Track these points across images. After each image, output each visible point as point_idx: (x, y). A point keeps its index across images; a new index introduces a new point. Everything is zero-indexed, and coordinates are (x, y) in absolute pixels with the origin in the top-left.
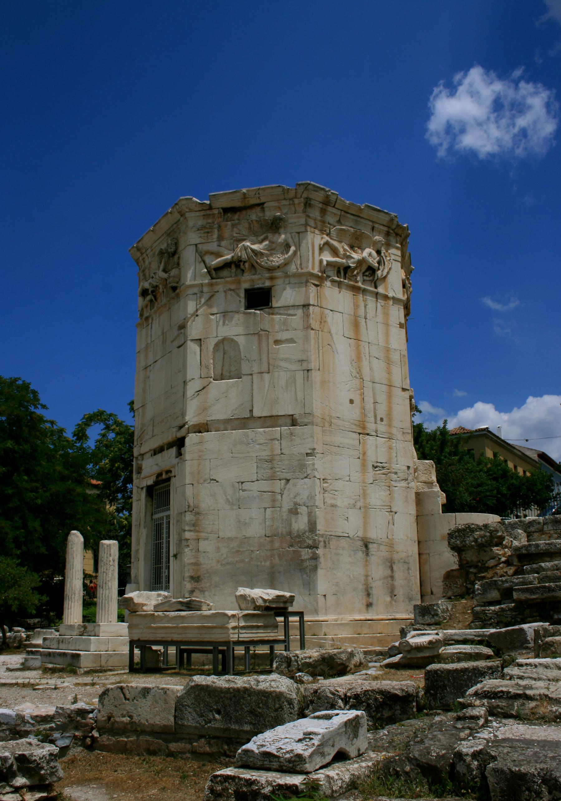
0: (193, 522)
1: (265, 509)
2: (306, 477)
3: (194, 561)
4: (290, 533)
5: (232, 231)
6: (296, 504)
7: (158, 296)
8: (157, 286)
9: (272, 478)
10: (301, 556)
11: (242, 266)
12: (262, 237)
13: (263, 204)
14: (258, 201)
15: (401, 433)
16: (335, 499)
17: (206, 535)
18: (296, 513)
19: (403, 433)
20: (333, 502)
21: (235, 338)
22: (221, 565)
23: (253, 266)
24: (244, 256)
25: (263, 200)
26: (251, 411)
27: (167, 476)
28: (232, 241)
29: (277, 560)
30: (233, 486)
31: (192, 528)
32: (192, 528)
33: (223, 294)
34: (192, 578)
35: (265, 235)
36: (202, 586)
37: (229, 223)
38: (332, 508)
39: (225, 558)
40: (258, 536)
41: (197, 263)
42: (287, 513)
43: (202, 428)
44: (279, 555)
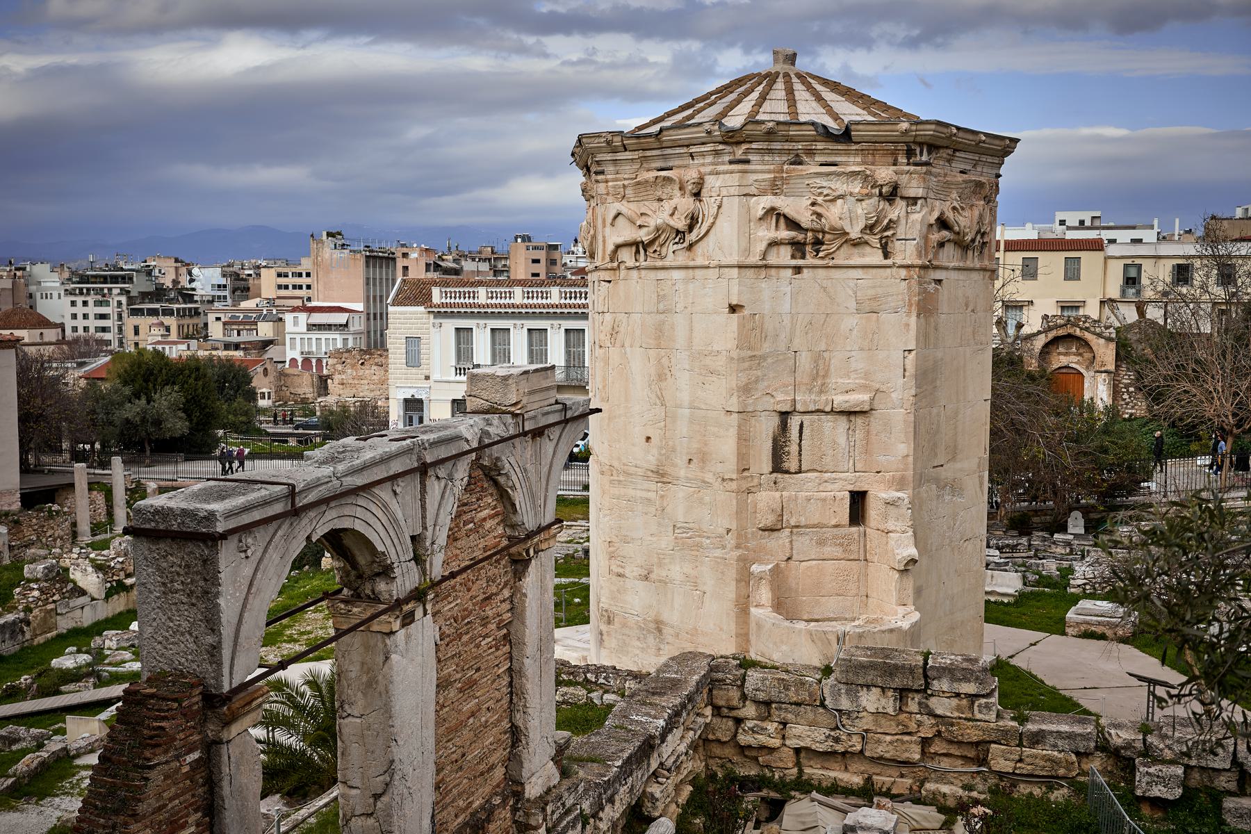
19: (723, 480)
20: (621, 570)
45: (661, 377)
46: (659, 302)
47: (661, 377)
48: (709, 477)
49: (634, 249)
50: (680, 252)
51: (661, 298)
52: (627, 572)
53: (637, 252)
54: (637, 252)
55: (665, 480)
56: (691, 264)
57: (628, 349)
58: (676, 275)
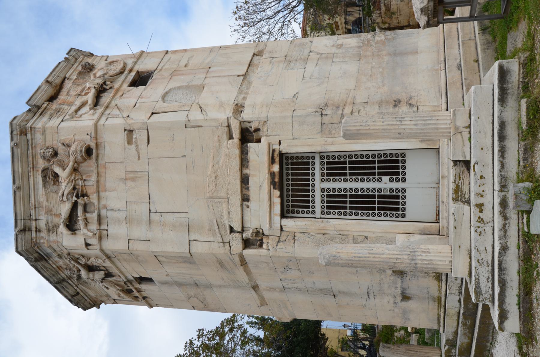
0: (334, 108)
1: (333, 62)
2: (312, 42)
3: (377, 105)
4: (359, 47)
6: (334, 45)
8: (74, 188)
10: (382, 40)
11: (108, 87)
21: (167, 90)
22: (383, 85)
24: (100, 81)
26: (238, 76)
27: (277, 160)
29: (384, 53)
32: (341, 108)
36: (405, 99)
43: (239, 109)
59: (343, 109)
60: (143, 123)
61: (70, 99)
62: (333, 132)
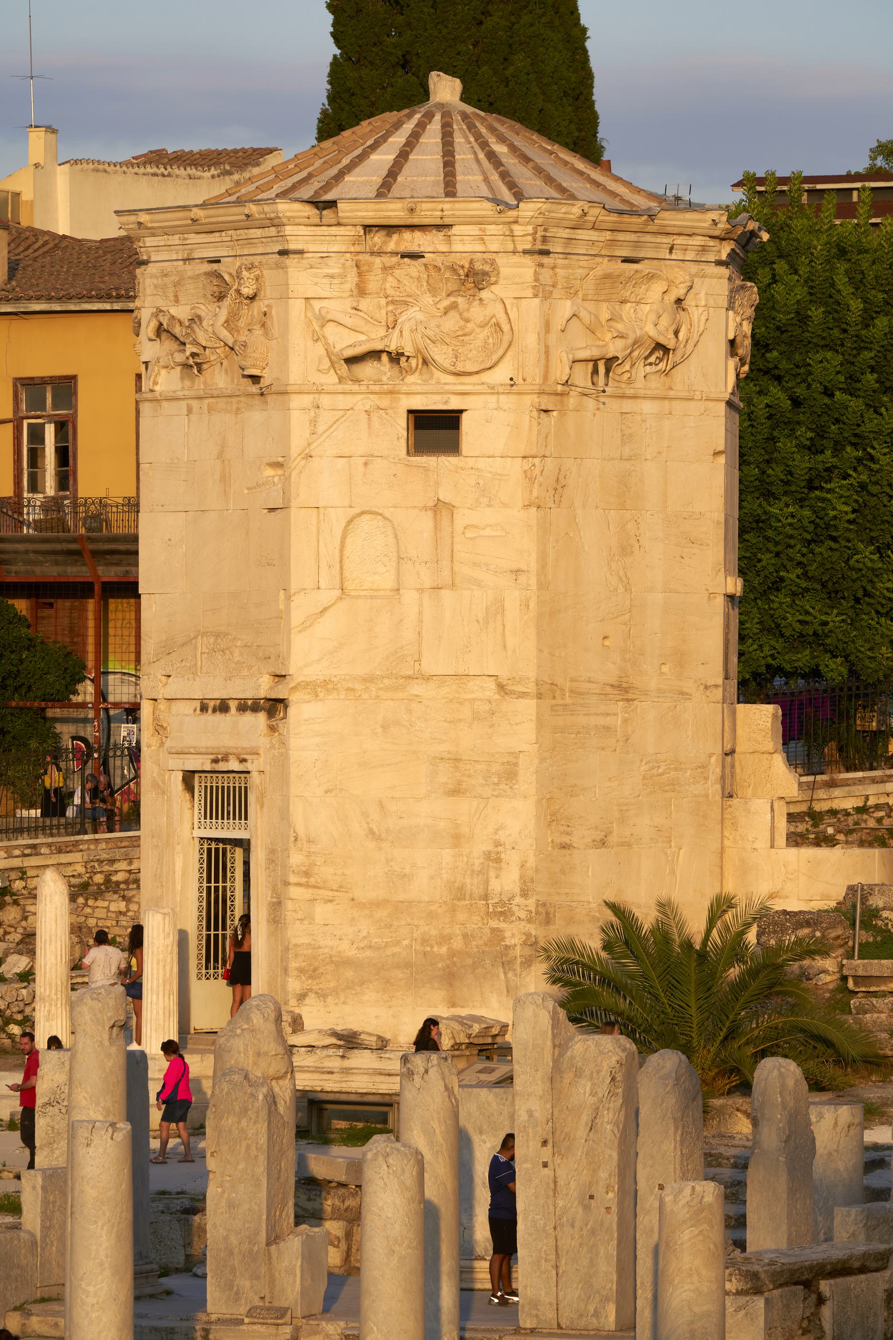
0: (304, 869)
4: (486, 897)
5: (384, 280)
6: (497, 844)
7: (205, 366)
9: (455, 791)
10: (503, 939)
12: (446, 303)
13: (449, 226)
14: (439, 222)
15: (702, 687)
16: (568, 834)
17: (331, 893)
18: (498, 860)
19: (706, 687)
20: (566, 839)
23: (425, 362)
25: (447, 221)
28: (383, 301)
30: (381, 805)
31: (304, 880)
32: (304, 880)
33: (364, 416)
34: (301, 970)
35: (452, 299)
37: (378, 261)
38: (564, 851)
39: (365, 938)
40: (427, 899)
41: (310, 343)
42: (481, 860)
44: (465, 936)
45: (625, 550)
46: (623, 443)
47: (625, 550)
48: (689, 686)
49: (591, 364)
50: (653, 377)
51: (627, 438)
52: (576, 840)
53: (595, 371)
54: (595, 371)
55: (630, 696)
56: (672, 394)
57: (579, 512)
58: (648, 407)
59: (298, 884)
60: (289, 501)
61: (373, 283)
62: (271, 866)
